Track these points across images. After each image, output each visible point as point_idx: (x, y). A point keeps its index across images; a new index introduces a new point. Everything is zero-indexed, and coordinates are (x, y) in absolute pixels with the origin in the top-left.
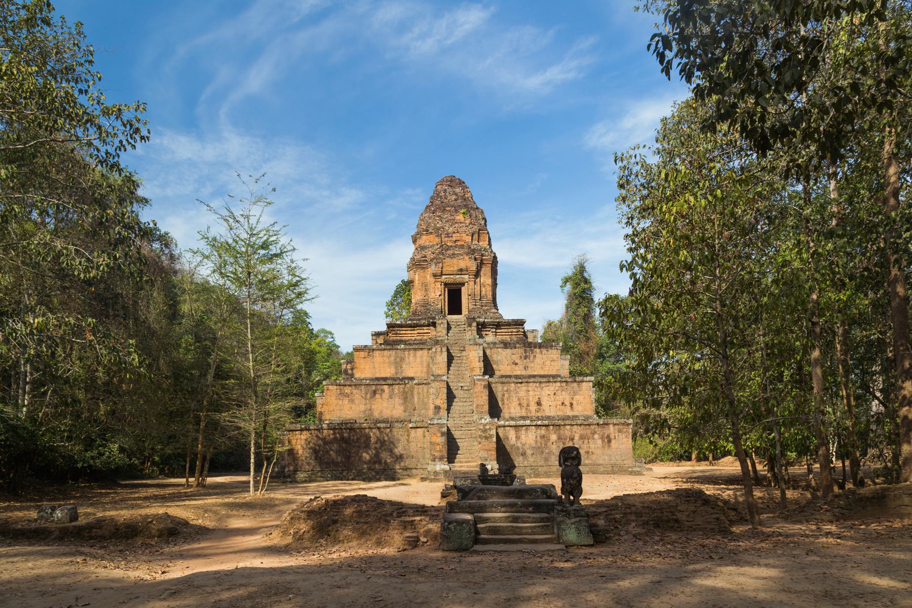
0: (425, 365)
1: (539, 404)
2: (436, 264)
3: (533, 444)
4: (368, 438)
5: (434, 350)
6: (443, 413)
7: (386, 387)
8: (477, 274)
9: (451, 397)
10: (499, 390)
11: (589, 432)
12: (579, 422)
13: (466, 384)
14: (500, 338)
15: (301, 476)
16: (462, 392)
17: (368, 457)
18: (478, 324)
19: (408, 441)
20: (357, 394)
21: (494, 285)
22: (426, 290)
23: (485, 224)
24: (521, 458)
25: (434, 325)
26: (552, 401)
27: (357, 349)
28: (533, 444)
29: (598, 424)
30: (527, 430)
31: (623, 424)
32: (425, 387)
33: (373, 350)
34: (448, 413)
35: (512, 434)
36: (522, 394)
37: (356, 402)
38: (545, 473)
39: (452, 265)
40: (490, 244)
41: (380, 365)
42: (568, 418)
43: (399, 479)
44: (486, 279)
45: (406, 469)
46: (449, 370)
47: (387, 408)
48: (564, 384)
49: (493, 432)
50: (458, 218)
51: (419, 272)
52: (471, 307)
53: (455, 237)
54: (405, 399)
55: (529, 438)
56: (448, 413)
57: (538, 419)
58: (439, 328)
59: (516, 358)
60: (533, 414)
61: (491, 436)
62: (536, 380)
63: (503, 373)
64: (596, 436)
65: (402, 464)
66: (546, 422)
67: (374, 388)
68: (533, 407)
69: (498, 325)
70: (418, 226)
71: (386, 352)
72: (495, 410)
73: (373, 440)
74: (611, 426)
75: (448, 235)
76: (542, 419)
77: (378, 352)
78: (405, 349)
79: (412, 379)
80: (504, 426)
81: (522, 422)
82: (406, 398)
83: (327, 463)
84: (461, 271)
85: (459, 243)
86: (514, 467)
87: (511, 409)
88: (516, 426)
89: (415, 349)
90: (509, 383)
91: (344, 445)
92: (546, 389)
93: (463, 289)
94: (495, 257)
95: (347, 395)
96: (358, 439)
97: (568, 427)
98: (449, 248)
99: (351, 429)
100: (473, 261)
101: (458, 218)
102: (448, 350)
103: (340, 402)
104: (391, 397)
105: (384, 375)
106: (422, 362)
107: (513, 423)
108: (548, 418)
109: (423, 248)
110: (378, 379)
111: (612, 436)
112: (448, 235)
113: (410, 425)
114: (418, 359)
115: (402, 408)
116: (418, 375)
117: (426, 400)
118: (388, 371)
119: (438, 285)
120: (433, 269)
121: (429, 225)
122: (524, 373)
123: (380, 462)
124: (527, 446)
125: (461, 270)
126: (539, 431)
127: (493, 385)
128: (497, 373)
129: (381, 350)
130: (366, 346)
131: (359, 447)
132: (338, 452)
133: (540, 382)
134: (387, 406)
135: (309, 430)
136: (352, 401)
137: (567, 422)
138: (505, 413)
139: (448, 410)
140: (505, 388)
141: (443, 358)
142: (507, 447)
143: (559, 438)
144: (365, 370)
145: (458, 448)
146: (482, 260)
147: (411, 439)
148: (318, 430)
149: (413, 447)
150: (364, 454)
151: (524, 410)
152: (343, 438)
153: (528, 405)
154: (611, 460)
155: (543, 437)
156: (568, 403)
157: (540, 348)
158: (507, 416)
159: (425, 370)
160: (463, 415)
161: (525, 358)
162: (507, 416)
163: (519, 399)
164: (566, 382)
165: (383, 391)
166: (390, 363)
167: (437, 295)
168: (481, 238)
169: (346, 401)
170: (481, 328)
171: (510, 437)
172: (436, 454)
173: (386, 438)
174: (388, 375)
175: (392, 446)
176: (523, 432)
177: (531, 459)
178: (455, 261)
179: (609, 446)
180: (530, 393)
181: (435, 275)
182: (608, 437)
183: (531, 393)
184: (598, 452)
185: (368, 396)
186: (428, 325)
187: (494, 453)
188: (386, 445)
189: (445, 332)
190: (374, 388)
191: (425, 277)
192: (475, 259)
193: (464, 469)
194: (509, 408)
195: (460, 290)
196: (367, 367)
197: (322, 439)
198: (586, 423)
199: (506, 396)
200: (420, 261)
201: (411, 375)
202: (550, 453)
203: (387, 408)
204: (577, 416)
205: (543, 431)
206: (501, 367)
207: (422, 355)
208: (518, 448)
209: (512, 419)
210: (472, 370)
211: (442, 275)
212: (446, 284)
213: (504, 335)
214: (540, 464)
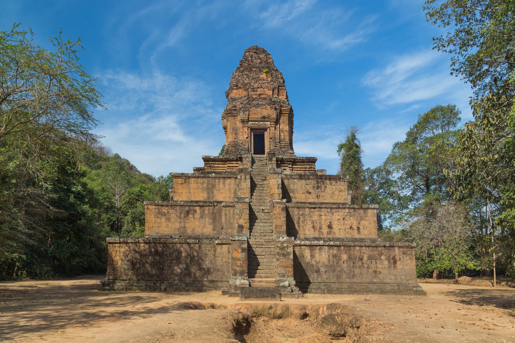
0: (232, 191)
1: (330, 227)
2: (244, 112)
3: (326, 262)
4: (180, 253)
6: (246, 231)
7: (197, 208)
8: (277, 122)
9: (253, 218)
10: (295, 213)
11: (376, 253)
12: (367, 244)
13: (266, 207)
14: (295, 172)
15: (119, 285)
16: (263, 214)
17: (179, 271)
18: (277, 160)
19: (214, 255)
20: (173, 214)
21: (291, 132)
23: (284, 82)
24: (315, 274)
25: (241, 159)
26: (342, 225)
27: (175, 176)
28: (326, 262)
29: (384, 246)
30: (320, 249)
31: (407, 247)
32: (231, 209)
34: (251, 232)
35: (307, 253)
36: (315, 218)
37: (172, 220)
38: (338, 289)
39: (257, 113)
40: (287, 98)
41: (196, 192)
42: (355, 240)
43: (206, 291)
44: (284, 126)
45: (213, 281)
46: (252, 195)
47: (199, 227)
48: (352, 211)
49: (291, 250)
50: (261, 76)
51: (231, 118)
52: (272, 148)
53: (260, 91)
54: (214, 219)
55: (323, 257)
56: (251, 232)
57: (329, 240)
58: (245, 162)
59: (310, 188)
60: (325, 236)
61: (288, 254)
62: (327, 206)
63: (298, 200)
64: (383, 257)
65: (210, 278)
66: (338, 243)
67: (187, 208)
68: (325, 230)
69: (294, 162)
70: (230, 84)
72: (291, 230)
73: (183, 255)
74: (396, 248)
75: (253, 90)
76: (334, 240)
77: (193, 179)
79: (221, 202)
80: (300, 245)
81: (316, 242)
82: (215, 218)
83: (143, 274)
85: (262, 96)
86: (309, 283)
87: (306, 231)
88: (310, 246)
89: (224, 178)
90: (304, 208)
91: (157, 258)
92: (336, 214)
93: (266, 133)
94: (291, 110)
95: (164, 214)
96: (170, 253)
97: (358, 248)
98: (254, 100)
99: (165, 244)
100: (274, 110)
101: (261, 76)
102: (251, 178)
103: (158, 220)
104: (202, 217)
106: (230, 190)
107: (308, 243)
108: (338, 239)
110: (192, 202)
111: (397, 258)
112: (253, 90)
113: (217, 242)
114: (227, 187)
115: (211, 227)
116: (227, 200)
117: (232, 220)
118: (201, 196)
119: (246, 129)
120: (242, 116)
121: (238, 82)
122: (316, 201)
123: (189, 274)
124: (321, 264)
125: (264, 117)
127: (290, 210)
128: (294, 200)
129: (195, 177)
130: (183, 174)
131: (172, 260)
132: (153, 264)
133: (331, 208)
134: (199, 225)
135: (127, 243)
136: (168, 220)
137: (357, 244)
138: (301, 234)
139: (251, 229)
140: (301, 213)
141: (247, 184)
142: (303, 264)
143: (350, 258)
144: (182, 194)
145: (258, 264)
146: (281, 110)
147: (217, 255)
148: (135, 243)
149: (219, 261)
150: (176, 268)
151: (317, 232)
152: (157, 252)
154: (397, 279)
155: (335, 256)
156: (355, 227)
157: (330, 179)
158: (302, 236)
159: (232, 196)
160: (263, 234)
161: (318, 188)
162: (302, 236)
163: (313, 223)
164: (354, 208)
165: (195, 211)
166: (203, 189)
167: (244, 136)
168: (280, 93)
169: (163, 220)
170: (280, 163)
171: (306, 255)
173: (195, 254)
174: (202, 199)
175: (200, 261)
176: (317, 251)
177: (325, 276)
178: (259, 110)
179: (395, 267)
180: (323, 217)
182: (394, 258)
183: (323, 217)
184: (385, 271)
185: (183, 215)
186: (237, 160)
187: (291, 270)
188: (195, 260)
189: (249, 165)
190: (187, 208)
191: (235, 123)
192: (276, 109)
193: (264, 284)
194: (304, 230)
195: (263, 135)
196: (184, 191)
197: (139, 253)
198: (373, 245)
199: (302, 219)
202: (342, 271)
203: (199, 227)
204: (363, 239)
205: (335, 251)
206: (297, 195)
208: (312, 266)
209: (307, 239)
210: (272, 195)
211: (248, 121)
213: (299, 169)
214: (332, 281)
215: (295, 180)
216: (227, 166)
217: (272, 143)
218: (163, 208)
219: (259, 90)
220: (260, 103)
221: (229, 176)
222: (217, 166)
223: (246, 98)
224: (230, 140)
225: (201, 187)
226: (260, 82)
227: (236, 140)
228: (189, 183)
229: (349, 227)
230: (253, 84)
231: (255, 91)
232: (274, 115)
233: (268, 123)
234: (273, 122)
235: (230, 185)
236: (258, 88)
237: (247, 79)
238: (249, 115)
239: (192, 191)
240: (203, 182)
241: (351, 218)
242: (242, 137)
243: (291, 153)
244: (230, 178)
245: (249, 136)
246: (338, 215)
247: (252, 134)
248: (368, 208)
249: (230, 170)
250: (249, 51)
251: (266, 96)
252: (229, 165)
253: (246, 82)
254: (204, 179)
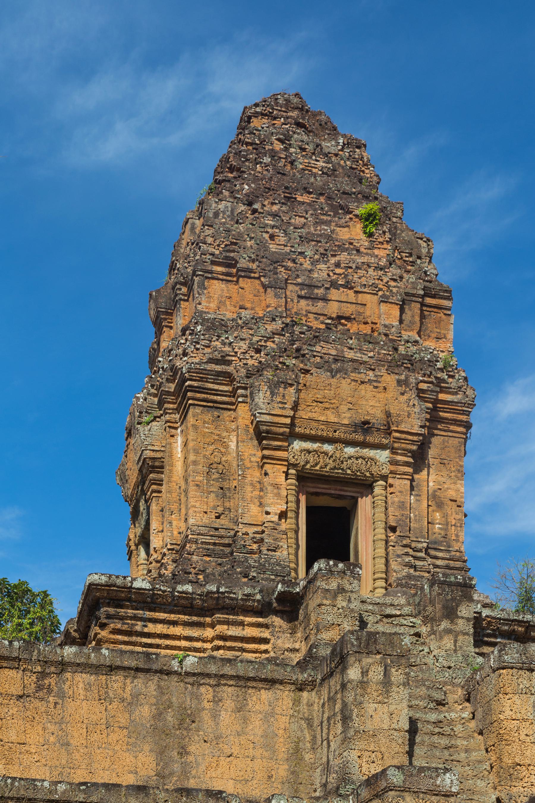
0: (283, 749)
2: (273, 387)
5: (353, 673)
22: (224, 493)
33: (63, 666)
53: (338, 302)
71: (117, 682)
75: (310, 292)
78: (198, 677)
84: (364, 432)
89: (243, 681)
93: (364, 504)
106: (268, 742)
112: (310, 292)
114: (256, 726)
119: (277, 473)
121: (234, 244)
125: (365, 426)
168: (430, 324)
178: (345, 386)
186: (263, 610)
196: (34, 737)
200: (202, 375)
207: (274, 707)
211: (293, 435)
216: (209, 633)
217: (400, 550)
219: (334, 294)
220: (350, 354)
221: (269, 672)
222: (159, 628)
223: (278, 325)
226: (343, 257)
227: (224, 522)
228: (61, 695)
230: (307, 265)
231: (316, 299)
233: (383, 456)
234: (406, 452)
235: (269, 716)
236: (334, 285)
237: (282, 239)
238: (295, 407)
239: (77, 737)
240: (136, 696)
242: (254, 509)
244: (271, 682)
245: (292, 505)
247: (303, 499)
249: (229, 654)
251: (367, 329)
252: (221, 629)
253: (273, 247)
254: (140, 682)
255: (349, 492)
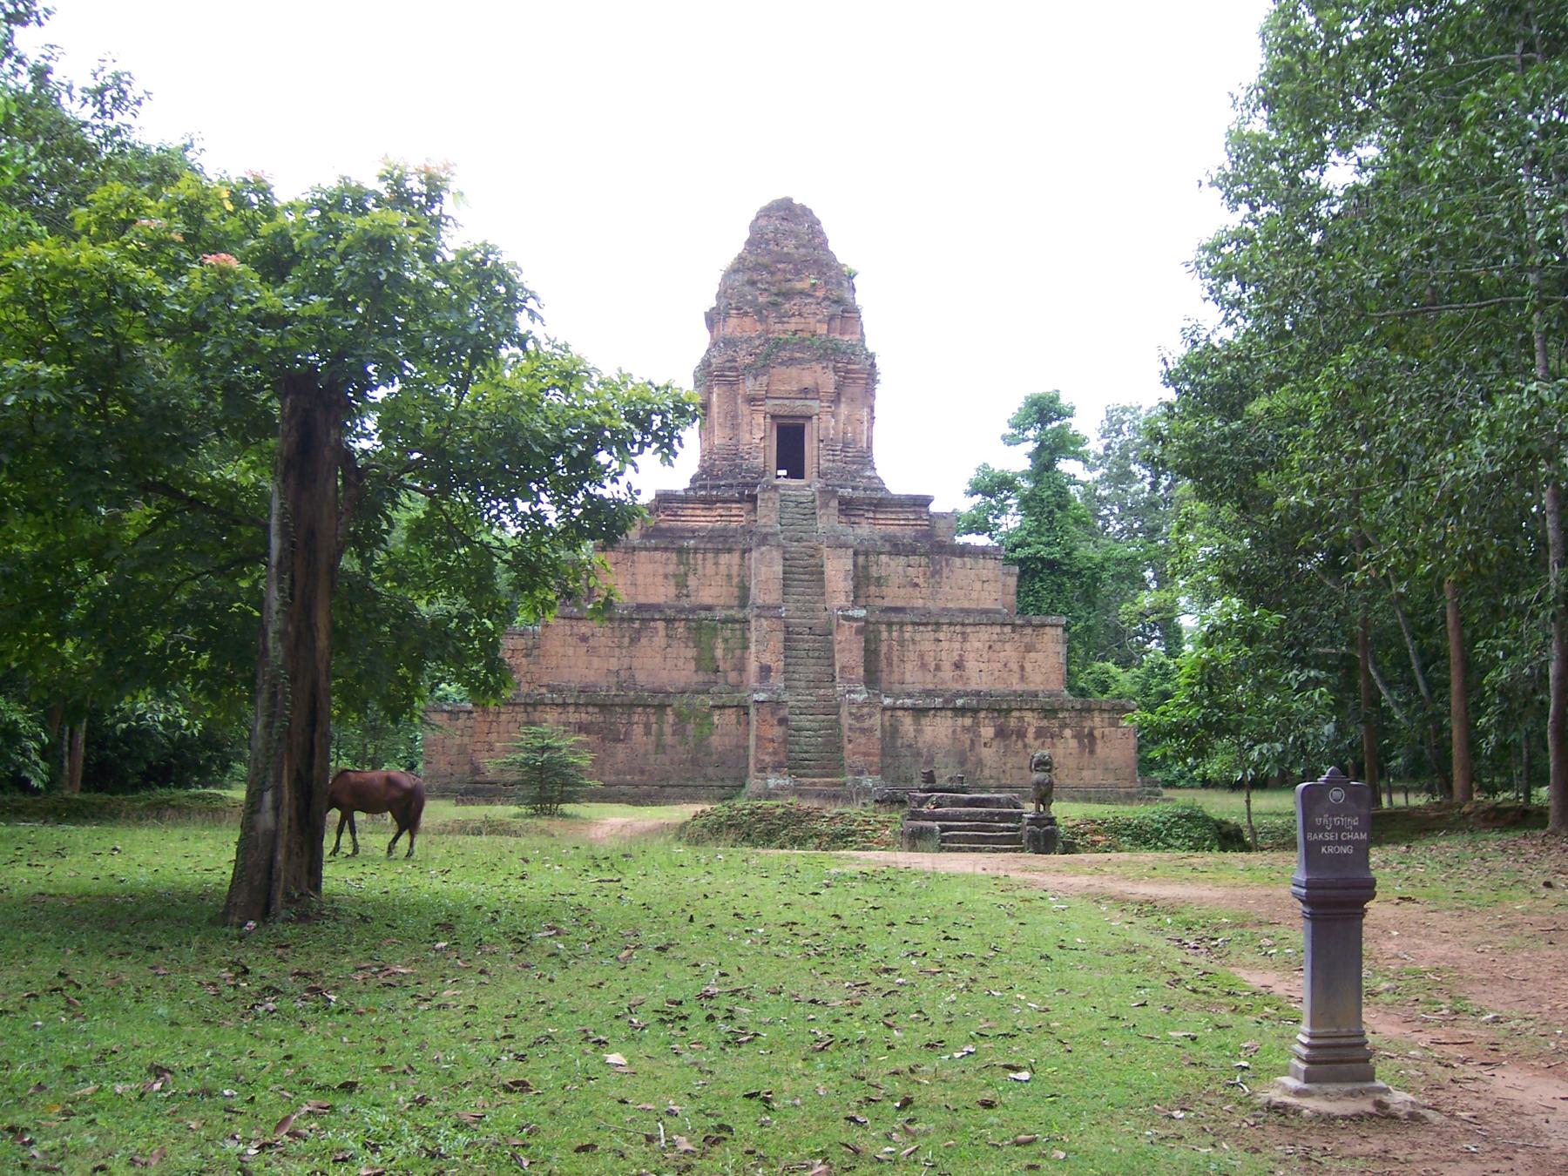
1: (958, 666)
33: (634, 549)
35: (907, 721)
64: (1068, 733)
68: (948, 673)
71: (658, 555)
74: (1096, 713)
80: (893, 709)
81: (928, 703)
105: (653, 600)
107: (908, 702)
108: (977, 694)
109: (729, 343)
111: (1097, 733)
118: (661, 593)
120: (749, 386)
126: (960, 721)
129: (646, 549)
136: (591, 651)
151: (929, 677)
153: (938, 668)
159: (736, 592)
161: (933, 576)
163: (921, 656)
167: (758, 438)
172: (767, 759)
178: (794, 371)
179: (1092, 752)
181: (752, 400)
182: (1091, 735)
183: (945, 645)
195: (803, 427)
201: (708, 601)
212: (773, 417)
215: (883, 557)
218: (581, 623)
222: (689, 512)
224: (718, 439)
225: (661, 571)
229: (999, 665)
232: (828, 381)
233: (815, 404)
239: (640, 579)
241: (1008, 646)
243: (870, 478)
246: (979, 639)
248: (1043, 626)
250: (766, 213)
255: (801, 421)
